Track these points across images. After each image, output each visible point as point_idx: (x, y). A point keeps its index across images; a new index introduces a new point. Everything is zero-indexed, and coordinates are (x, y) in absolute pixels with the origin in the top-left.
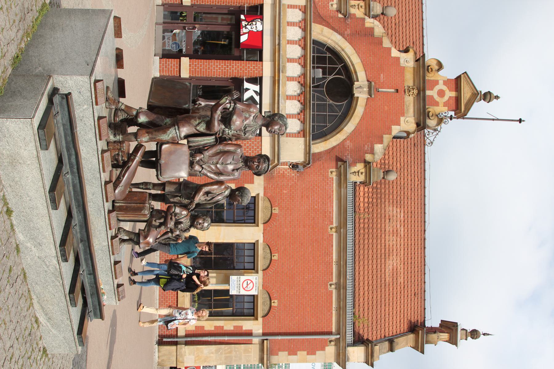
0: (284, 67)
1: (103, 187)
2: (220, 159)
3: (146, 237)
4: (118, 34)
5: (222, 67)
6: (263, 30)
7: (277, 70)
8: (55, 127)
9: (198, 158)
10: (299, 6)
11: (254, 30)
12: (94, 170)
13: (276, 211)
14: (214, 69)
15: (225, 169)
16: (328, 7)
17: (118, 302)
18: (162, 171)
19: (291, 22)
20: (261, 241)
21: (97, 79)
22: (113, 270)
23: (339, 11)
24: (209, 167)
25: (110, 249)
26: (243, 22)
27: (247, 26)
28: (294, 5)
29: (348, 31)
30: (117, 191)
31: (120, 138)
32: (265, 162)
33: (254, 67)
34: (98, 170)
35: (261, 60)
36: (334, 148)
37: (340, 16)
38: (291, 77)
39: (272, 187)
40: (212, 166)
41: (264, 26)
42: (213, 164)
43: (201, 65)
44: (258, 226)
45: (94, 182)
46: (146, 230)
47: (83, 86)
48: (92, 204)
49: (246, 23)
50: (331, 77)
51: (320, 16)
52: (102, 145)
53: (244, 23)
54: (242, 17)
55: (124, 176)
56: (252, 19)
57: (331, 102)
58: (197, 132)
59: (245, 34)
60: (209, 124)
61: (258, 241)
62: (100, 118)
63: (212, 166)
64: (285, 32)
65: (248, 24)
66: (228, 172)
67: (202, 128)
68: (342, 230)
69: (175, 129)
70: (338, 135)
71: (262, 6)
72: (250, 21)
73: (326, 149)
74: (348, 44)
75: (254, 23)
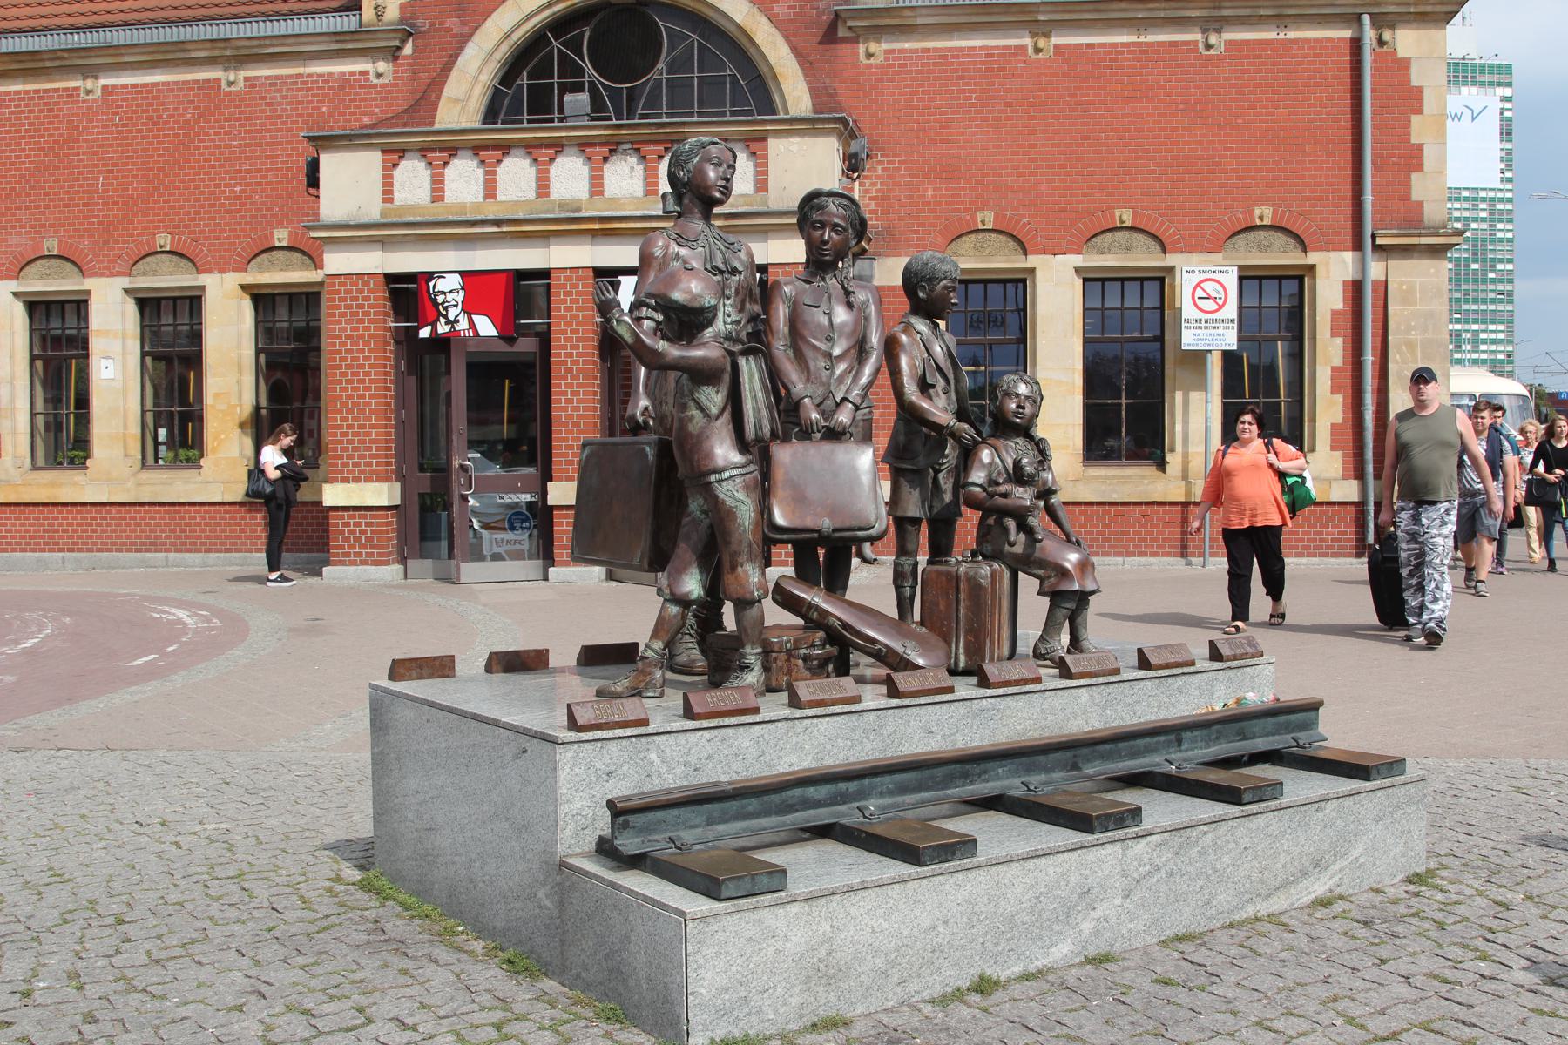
0: (562, 205)
1: (907, 702)
2: (815, 348)
3: (1064, 573)
4: (443, 667)
5: (571, 386)
6: (463, 274)
7: (573, 226)
8: (718, 848)
9: (814, 415)
10: (384, 169)
11: (460, 297)
12: (854, 728)
13: (987, 218)
14: (578, 409)
15: (848, 329)
16: (383, 86)
17: (1265, 659)
18: (855, 524)
19: (433, 190)
20: (1077, 260)
21: (563, 719)
23: (394, 54)
24: (841, 380)
25: (1101, 680)
26: (440, 330)
27: (451, 317)
28: (384, 185)
29: (452, 22)
30: (920, 662)
31: (752, 654)
32: (822, 207)
33: (566, 294)
34: (854, 717)
35: (544, 274)
36: (795, 50)
37: (408, 49)
38: (592, 185)
39: (916, 232)
40: (838, 372)
41: (447, 268)
42: (832, 369)
43: (568, 447)
44: (1032, 271)
46: (1041, 572)
47: (590, 766)
48: (959, 737)
49: (442, 320)
50: (589, 68)
51: (413, 109)
52: (774, 706)
53: (443, 328)
54: (425, 333)
55: (873, 641)
56: (428, 304)
57: (661, 65)
58: (727, 414)
59: (472, 325)
60: (702, 375)
61: (1078, 270)
62: (689, 713)
63: (838, 372)
64: (463, 206)
65: (446, 317)
66: (857, 322)
67: (714, 398)
68: (1042, 18)
69: (719, 481)
70: (759, 39)
71: (391, 278)
72: (436, 311)
73: (800, 73)
74: (489, 22)
75: (440, 299)
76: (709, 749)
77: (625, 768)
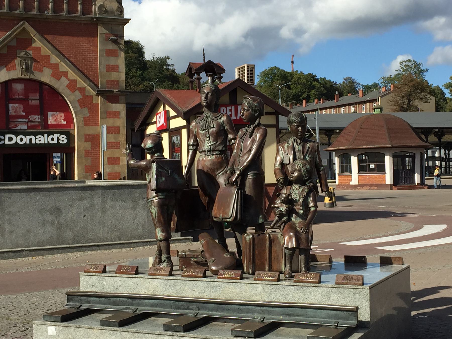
22: (302, 284)
34: (166, 281)
45: (179, 287)
47: (87, 282)
76: (120, 283)
77: (97, 285)
